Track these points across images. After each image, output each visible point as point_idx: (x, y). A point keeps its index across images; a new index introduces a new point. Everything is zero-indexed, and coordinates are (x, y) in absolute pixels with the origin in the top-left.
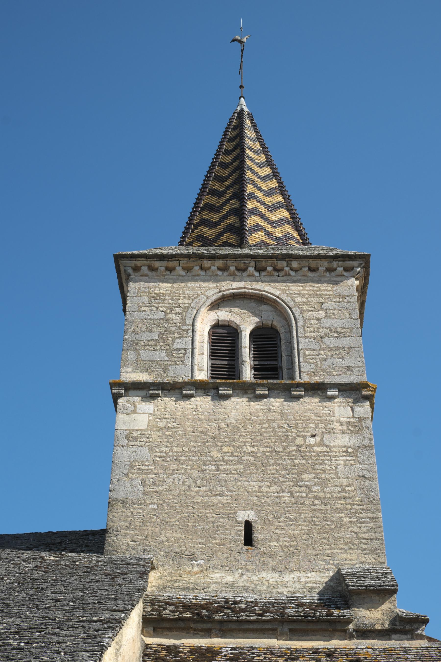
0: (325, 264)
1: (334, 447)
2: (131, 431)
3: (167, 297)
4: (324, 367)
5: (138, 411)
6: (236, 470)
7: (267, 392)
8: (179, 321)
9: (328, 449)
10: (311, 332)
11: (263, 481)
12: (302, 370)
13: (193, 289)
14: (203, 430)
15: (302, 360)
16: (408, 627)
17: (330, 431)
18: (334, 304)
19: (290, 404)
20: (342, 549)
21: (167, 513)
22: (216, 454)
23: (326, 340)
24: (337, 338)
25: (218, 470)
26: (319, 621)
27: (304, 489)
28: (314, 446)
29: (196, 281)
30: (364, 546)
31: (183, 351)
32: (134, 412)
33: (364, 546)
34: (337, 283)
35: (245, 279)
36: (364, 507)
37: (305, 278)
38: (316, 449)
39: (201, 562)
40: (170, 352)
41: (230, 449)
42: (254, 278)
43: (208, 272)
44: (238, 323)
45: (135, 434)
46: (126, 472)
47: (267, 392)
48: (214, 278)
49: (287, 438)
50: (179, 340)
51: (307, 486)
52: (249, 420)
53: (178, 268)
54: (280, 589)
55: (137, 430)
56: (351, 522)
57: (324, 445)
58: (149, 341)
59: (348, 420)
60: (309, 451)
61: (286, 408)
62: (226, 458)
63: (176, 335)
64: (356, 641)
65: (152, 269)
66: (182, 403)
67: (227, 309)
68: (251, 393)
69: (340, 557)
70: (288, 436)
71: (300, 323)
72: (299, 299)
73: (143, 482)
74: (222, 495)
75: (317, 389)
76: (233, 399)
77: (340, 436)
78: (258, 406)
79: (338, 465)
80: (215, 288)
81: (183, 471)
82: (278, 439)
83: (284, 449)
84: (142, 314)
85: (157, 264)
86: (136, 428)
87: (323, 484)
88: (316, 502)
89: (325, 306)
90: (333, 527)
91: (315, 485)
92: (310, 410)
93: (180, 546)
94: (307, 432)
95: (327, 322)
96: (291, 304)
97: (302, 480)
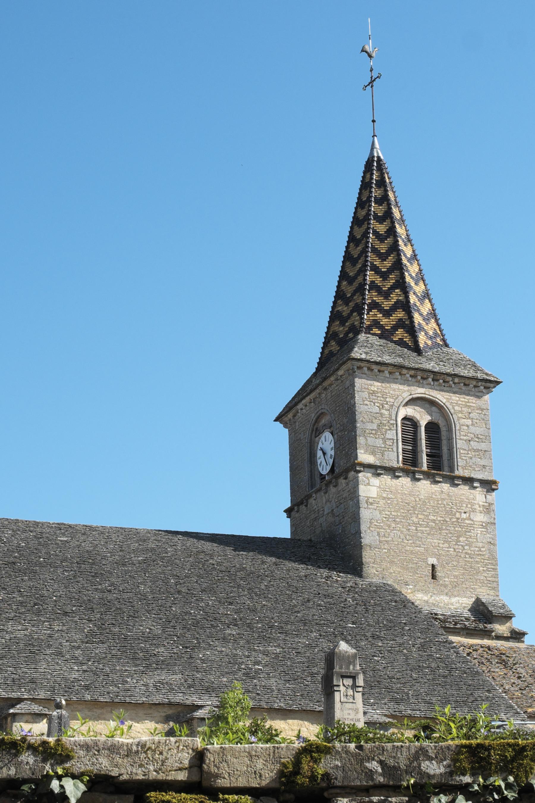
0: (474, 383)
1: (476, 521)
2: (368, 498)
3: (379, 395)
4: (471, 464)
5: (371, 484)
6: (426, 531)
7: (441, 480)
8: (388, 416)
9: (472, 523)
10: (464, 436)
11: (440, 540)
12: (459, 464)
13: (394, 390)
14: (407, 501)
15: (458, 457)
16: (518, 636)
17: (474, 511)
18: (477, 415)
19: (453, 488)
20: (479, 586)
21: (393, 555)
22: (415, 520)
23: (472, 443)
24: (478, 442)
25: (416, 530)
26: (481, 630)
27: (460, 547)
28: (465, 519)
29: (396, 383)
30: (489, 585)
31: (392, 441)
32: (368, 484)
33: (489, 585)
34: (479, 397)
35: (426, 386)
36: (490, 562)
37: (460, 391)
38: (467, 521)
39: (411, 587)
40: (384, 440)
41: (422, 517)
42: (430, 386)
43: (403, 376)
44: (418, 419)
45: (371, 500)
46: (368, 526)
47: (441, 480)
48: (405, 382)
49: (452, 513)
50: (389, 432)
51: (462, 546)
52: (431, 497)
53: (386, 372)
54: (450, 606)
55: (372, 497)
56: (483, 570)
57: (470, 519)
58: (372, 430)
59: (483, 504)
60: (463, 523)
61: (451, 491)
62: (420, 522)
63: (387, 427)
64: (494, 641)
65: (369, 369)
66: (394, 480)
67: (412, 407)
68: (432, 478)
69: (478, 590)
70: (452, 511)
71: (457, 428)
72: (457, 408)
73: (378, 534)
74: (420, 547)
75: (469, 481)
76: (422, 481)
77: (479, 514)
78: (436, 488)
79: (478, 533)
80: (408, 391)
81: (398, 529)
82: (447, 512)
83: (450, 520)
84: (366, 407)
85: (374, 367)
86: (371, 496)
87: (470, 545)
88: (467, 556)
89: (471, 415)
90: (475, 572)
91: (466, 545)
92: (463, 494)
93: (401, 577)
94: (462, 509)
95: (473, 429)
96: (452, 411)
97: (460, 541)
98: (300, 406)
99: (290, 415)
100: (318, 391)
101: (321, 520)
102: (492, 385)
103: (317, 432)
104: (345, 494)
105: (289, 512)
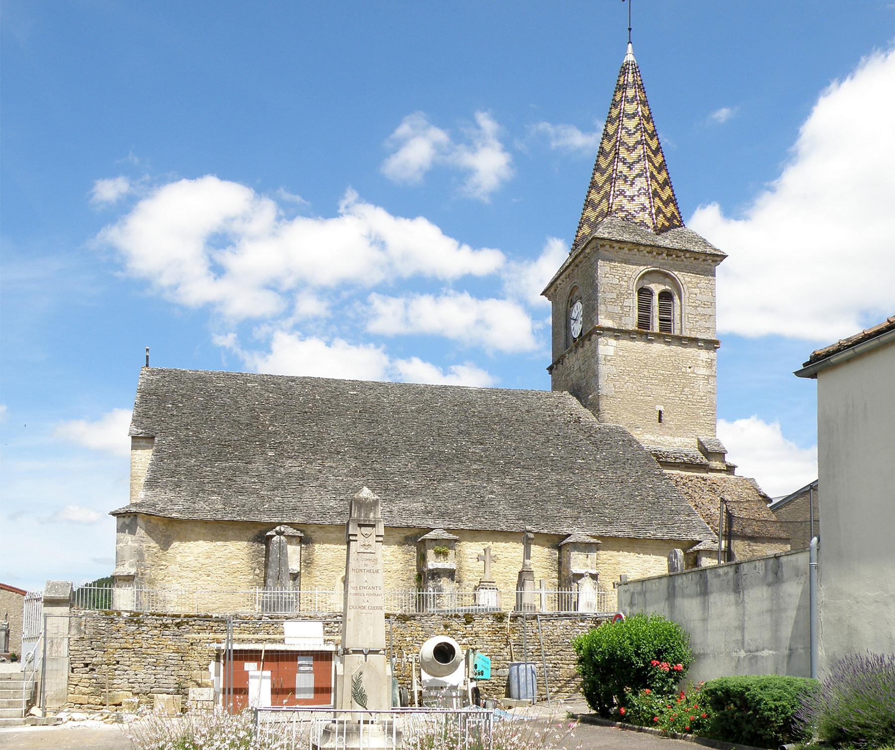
32: (607, 344)
45: (609, 358)
65: (611, 246)
85: (615, 245)
96: (683, 282)
98: (559, 282)
99: (552, 290)
100: (571, 268)
101: (573, 375)
102: (719, 259)
103: (572, 304)
104: (589, 354)
105: (550, 369)
